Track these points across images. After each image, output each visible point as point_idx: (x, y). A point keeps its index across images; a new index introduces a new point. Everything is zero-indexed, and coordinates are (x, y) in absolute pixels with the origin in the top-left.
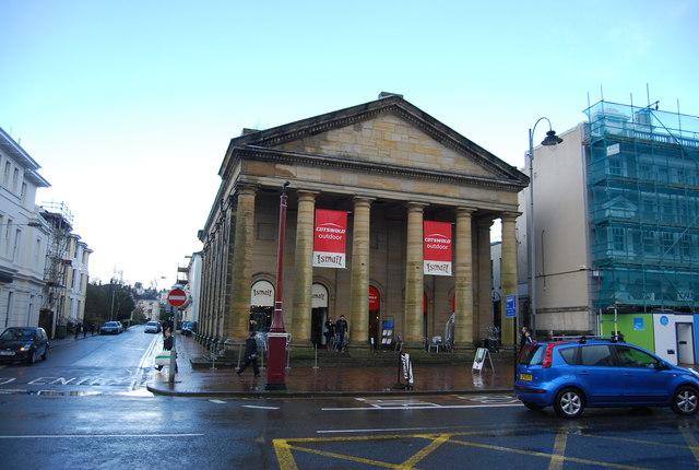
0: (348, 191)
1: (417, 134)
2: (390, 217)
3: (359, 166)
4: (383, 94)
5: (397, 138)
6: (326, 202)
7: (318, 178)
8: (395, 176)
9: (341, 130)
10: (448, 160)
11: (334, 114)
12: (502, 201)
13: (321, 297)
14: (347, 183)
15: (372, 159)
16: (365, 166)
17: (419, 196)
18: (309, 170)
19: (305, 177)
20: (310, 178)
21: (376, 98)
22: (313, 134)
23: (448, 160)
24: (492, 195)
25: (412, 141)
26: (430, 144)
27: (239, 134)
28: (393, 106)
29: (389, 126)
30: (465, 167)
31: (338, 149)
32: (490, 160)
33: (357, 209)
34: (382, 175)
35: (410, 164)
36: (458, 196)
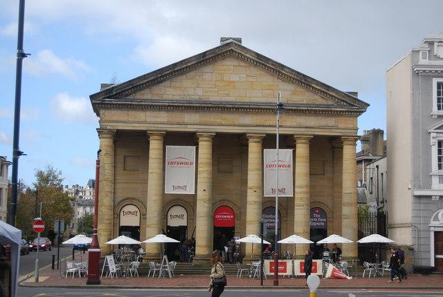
0: (191, 129)
1: (255, 71)
2: (230, 150)
3: (199, 107)
4: (222, 40)
5: (235, 78)
6: (172, 138)
7: (165, 120)
8: (233, 113)
9: (184, 77)
10: (286, 93)
11: (175, 65)
12: (341, 126)
13: (181, 217)
14: (189, 122)
15: (212, 99)
16: (205, 107)
17: (257, 128)
18: (156, 113)
19: (153, 120)
20: (158, 120)
21: (218, 44)
22: (159, 83)
23: (286, 93)
24: (331, 121)
25: (250, 79)
26: (267, 80)
27: (98, 90)
28: (229, 51)
29: (230, 70)
30: (303, 97)
31: (181, 93)
32: (325, 90)
33: (200, 143)
34: (222, 112)
35: (247, 100)
36: (295, 124)
